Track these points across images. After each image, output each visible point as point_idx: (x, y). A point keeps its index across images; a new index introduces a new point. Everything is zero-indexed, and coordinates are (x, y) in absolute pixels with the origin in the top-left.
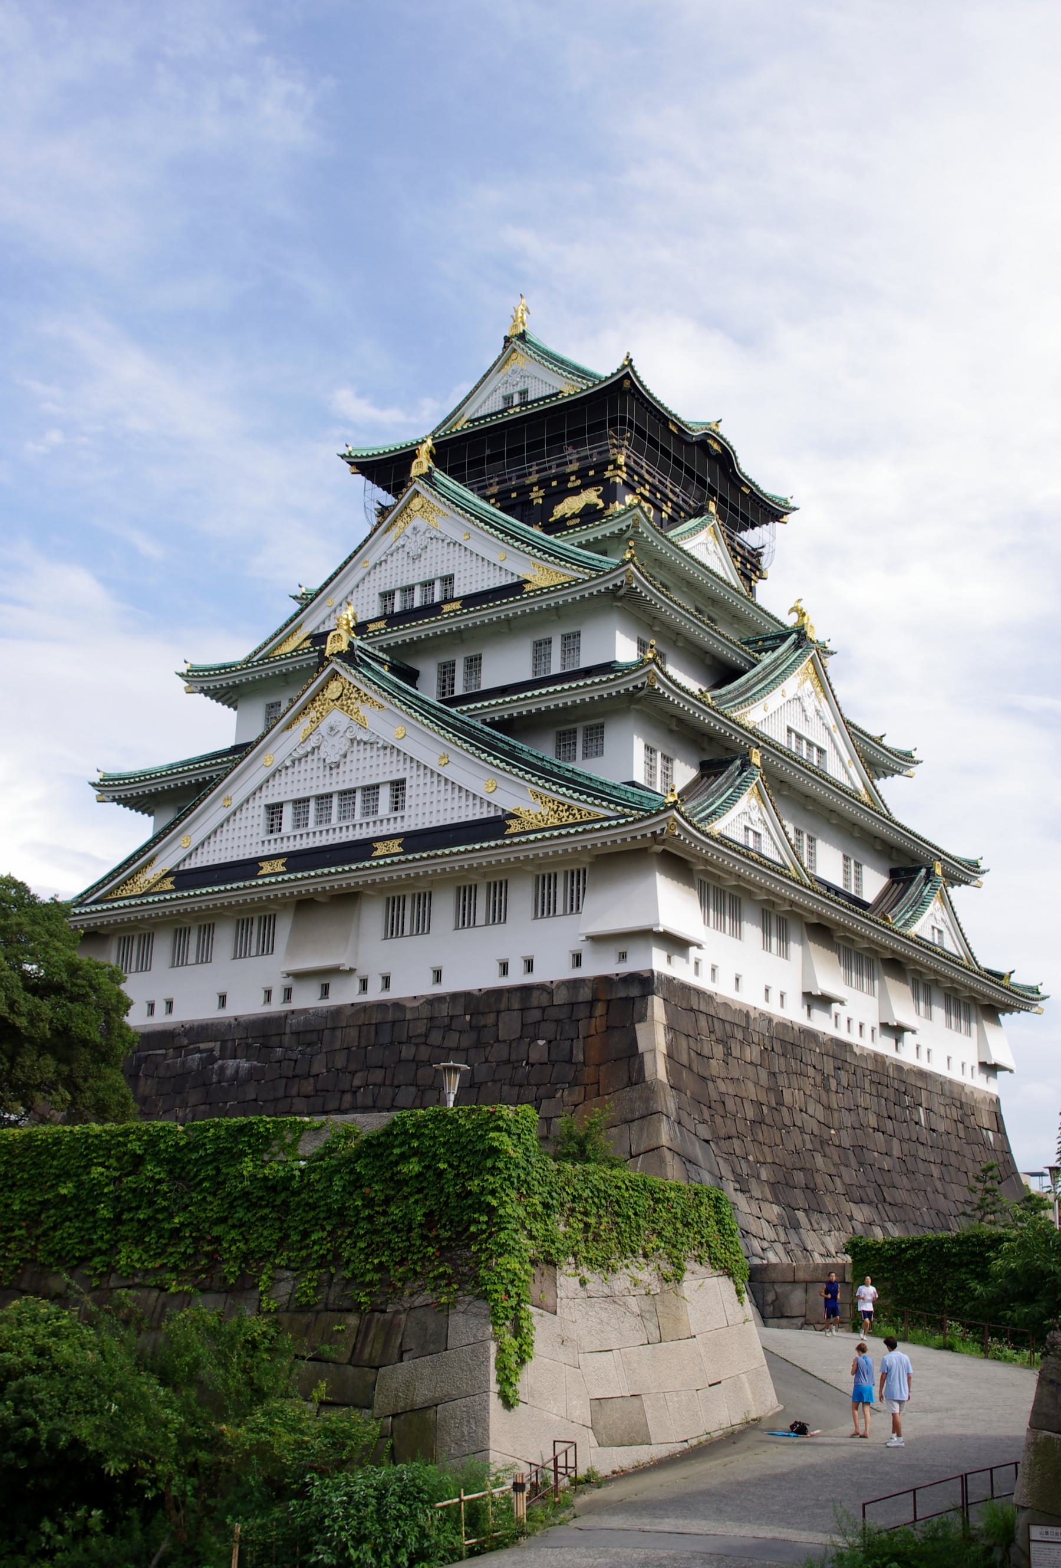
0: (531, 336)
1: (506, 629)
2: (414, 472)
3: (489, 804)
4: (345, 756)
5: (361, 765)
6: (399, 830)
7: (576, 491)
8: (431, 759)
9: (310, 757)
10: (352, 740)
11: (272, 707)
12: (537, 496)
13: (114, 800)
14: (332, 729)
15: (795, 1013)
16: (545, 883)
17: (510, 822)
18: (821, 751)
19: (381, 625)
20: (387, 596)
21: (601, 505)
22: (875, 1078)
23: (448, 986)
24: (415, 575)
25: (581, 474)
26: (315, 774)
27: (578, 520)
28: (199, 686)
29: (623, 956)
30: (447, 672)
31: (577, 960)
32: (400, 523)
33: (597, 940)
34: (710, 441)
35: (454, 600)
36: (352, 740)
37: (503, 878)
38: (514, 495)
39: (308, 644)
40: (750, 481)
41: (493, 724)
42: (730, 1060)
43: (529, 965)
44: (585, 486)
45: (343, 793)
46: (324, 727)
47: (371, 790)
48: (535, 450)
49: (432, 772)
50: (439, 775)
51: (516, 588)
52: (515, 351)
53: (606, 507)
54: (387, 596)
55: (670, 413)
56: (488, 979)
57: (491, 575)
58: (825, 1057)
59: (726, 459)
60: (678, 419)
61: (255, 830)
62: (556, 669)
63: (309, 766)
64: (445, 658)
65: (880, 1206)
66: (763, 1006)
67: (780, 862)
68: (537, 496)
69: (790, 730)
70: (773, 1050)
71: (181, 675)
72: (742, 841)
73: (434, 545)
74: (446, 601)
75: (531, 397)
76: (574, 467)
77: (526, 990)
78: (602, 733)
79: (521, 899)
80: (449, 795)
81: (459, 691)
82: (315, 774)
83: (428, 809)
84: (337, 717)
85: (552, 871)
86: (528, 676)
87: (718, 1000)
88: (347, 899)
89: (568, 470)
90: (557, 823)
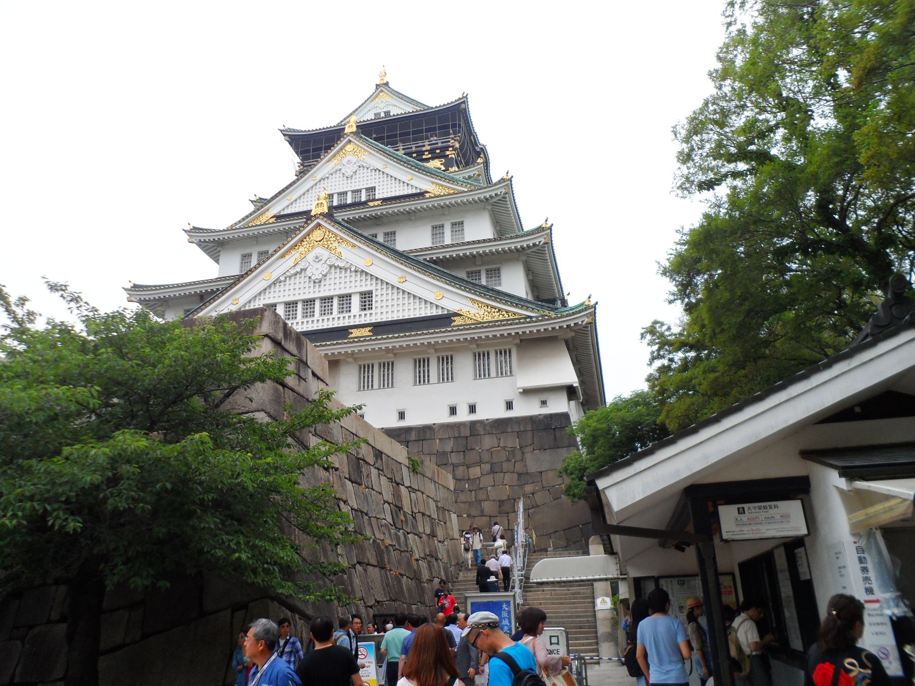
0: (390, 85)
1: (411, 217)
3: (437, 306)
4: (326, 276)
5: (337, 281)
6: (368, 322)
7: (427, 160)
8: (394, 280)
9: (298, 276)
10: (331, 267)
11: (246, 257)
14: (317, 257)
16: (481, 356)
17: (455, 318)
21: (443, 168)
23: (412, 421)
25: (430, 152)
26: (302, 286)
28: (198, 239)
29: (544, 403)
31: (509, 405)
32: (338, 157)
33: (527, 392)
35: (374, 200)
36: (331, 267)
37: (449, 354)
43: (472, 409)
44: (433, 158)
45: (323, 299)
46: (310, 257)
47: (345, 299)
48: (405, 137)
49: (393, 287)
50: (398, 288)
52: (382, 91)
56: (442, 417)
57: (401, 188)
62: (448, 240)
63: (297, 281)
71: (185, 231)
74: (370, 201)
76: (428, 148)
77: (473, 424)
78: (499, 273)
79: (464, 366)
80: (406, 301)
82: (302, 286)
84: (319, 251)
85: (486, 350)
86: (429, 245)
89: (424, 149)
90: (490, 319)
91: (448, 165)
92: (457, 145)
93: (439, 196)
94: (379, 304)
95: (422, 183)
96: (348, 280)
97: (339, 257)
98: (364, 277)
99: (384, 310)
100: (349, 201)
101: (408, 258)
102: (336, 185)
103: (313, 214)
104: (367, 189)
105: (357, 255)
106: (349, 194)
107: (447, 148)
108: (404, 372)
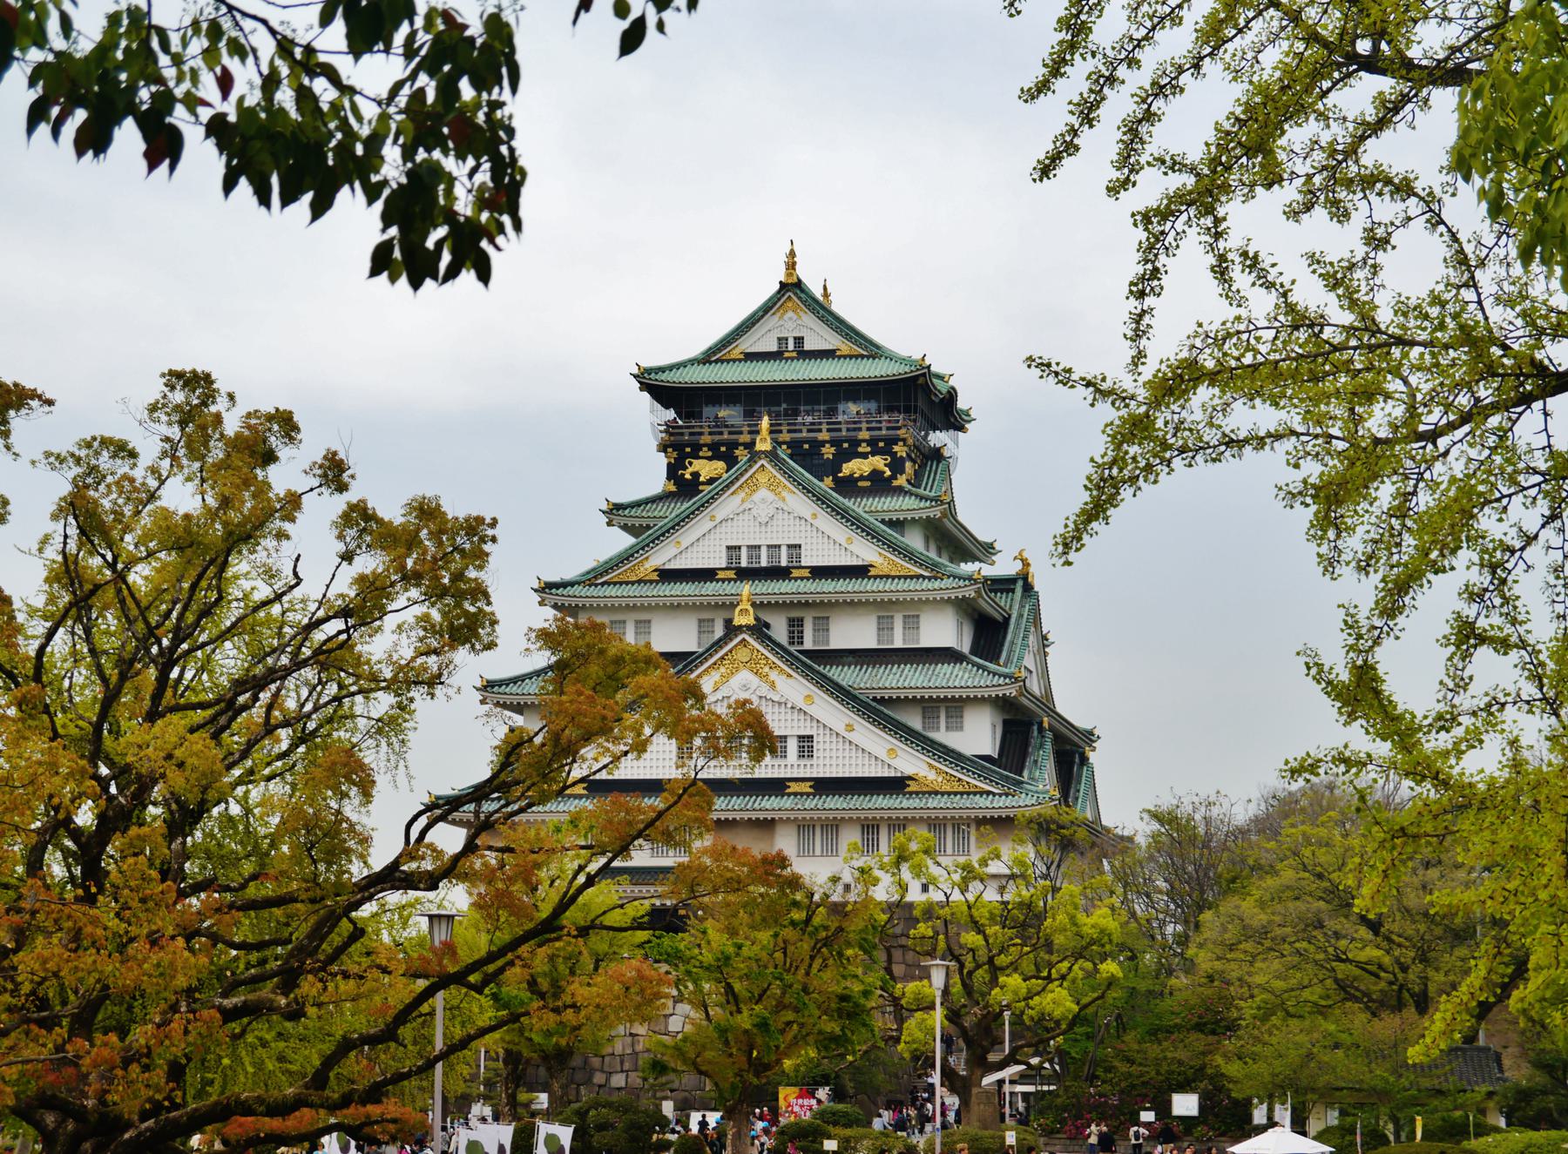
2: (760, 446)
7: (864, 456)
12: (828, 452)
13: (497, 704)
19: (731, 574)
20: (733, 549)
21: (888, 473)
24: (763, 540)
25: (872, 442)
27: (868, 484)
30: (796, 626)
38: (806, 446)
39: (655, 576)
41: (882, 701)
44: (873, 454)
51: (860, 572)
53: (894, 477)
54: (733, 549)
61: (667, 756)
62: (898, 643)
64: (795, 614)
68: (828, 452)
73: (780, 516)
75: (807, 347)
81: (808, 644)
83: (831, 763)
84: (745, 676)
86: (873, 644)
88: (767, 826)
90: (948, 789)
91: (897, 466)
92: (910, 441)
93: (887, 577)
94: (821, 754)
95: (864, 552)
96: (782, 717)
97: (773, 685)
98: (802, 717)
99: (827, 762)
100: (764, 563)
101: (854, 698)
102: (745, 533)
103: (736, 622)
104: (789, 546)
105: (793, 688)
106: (764, 551)
107: (895, 441)
108: (850, 837)
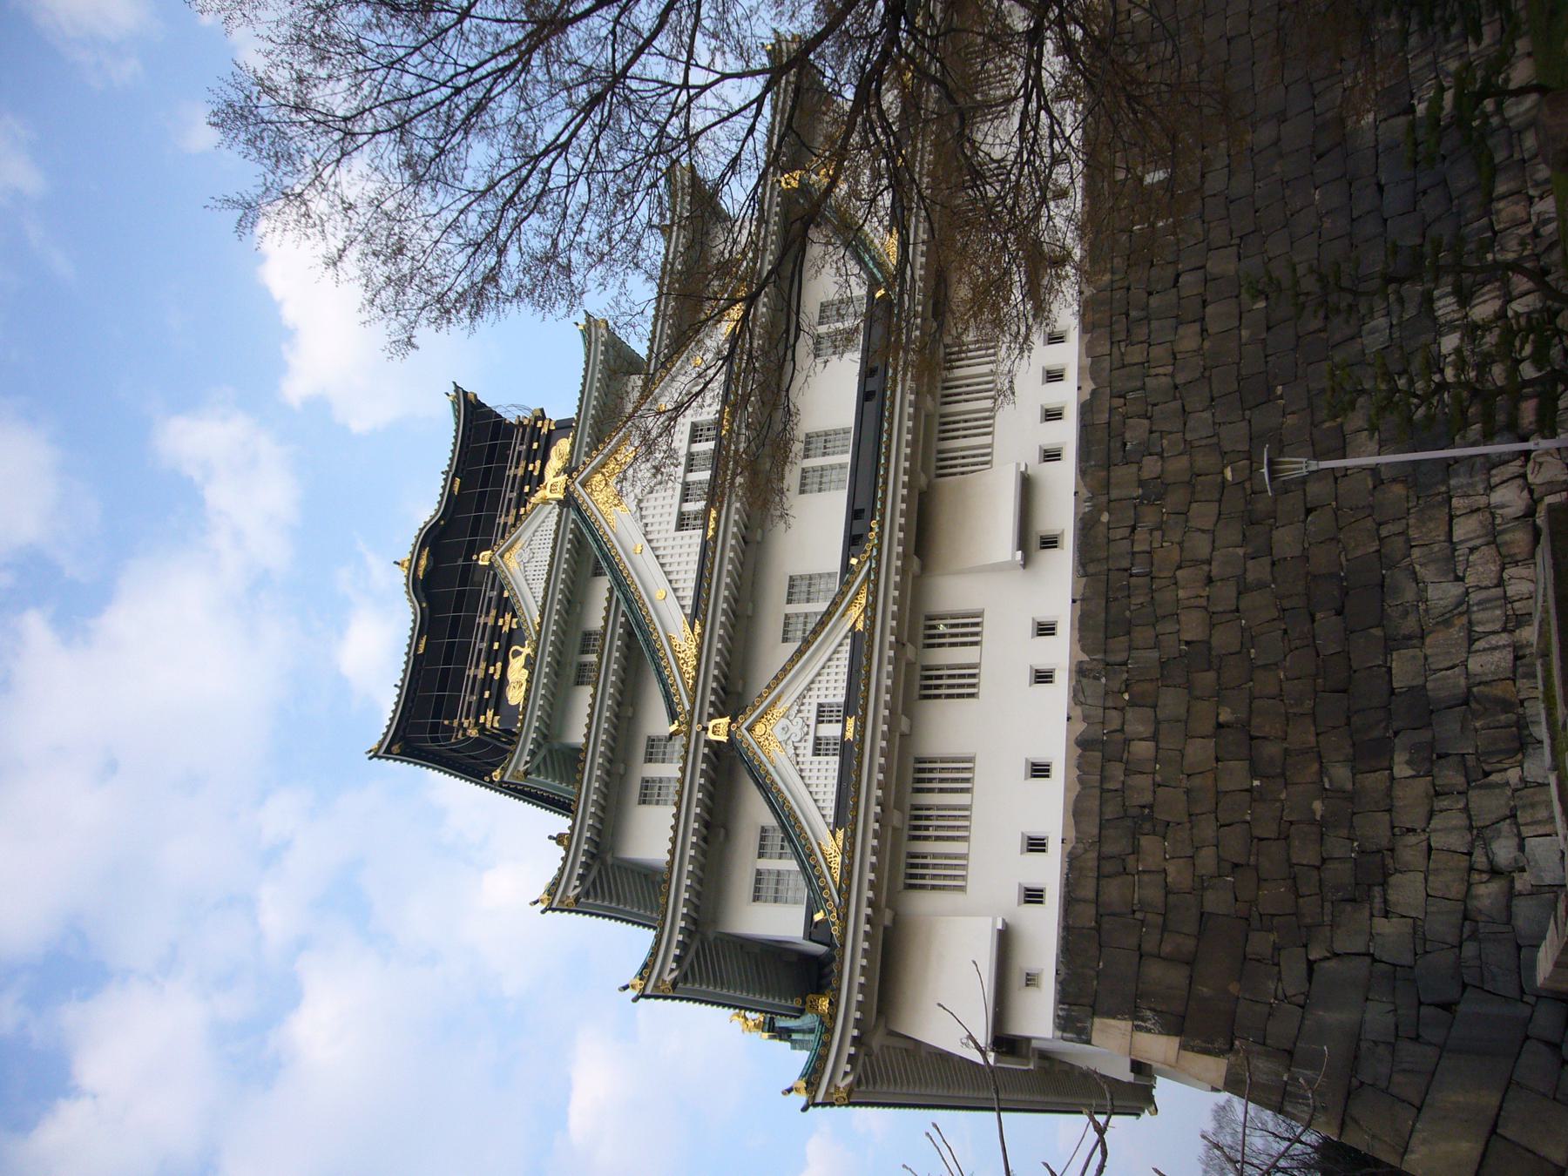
15: (1055, 586)
18: (696, 434)
22: (1120, 326)
34: (421, 574)
40: (444, 488)
42: (1162, 816)
55: (407, 663)
58: (1114, 494)
59: (434, 539)
60: (410, 646)
65: (1338, 357)
66: (1059, 692)
67: (847, 648)
69: (682, 523)
70: (1125, 664)
72: (834, 761)
87: (1072, 834)
